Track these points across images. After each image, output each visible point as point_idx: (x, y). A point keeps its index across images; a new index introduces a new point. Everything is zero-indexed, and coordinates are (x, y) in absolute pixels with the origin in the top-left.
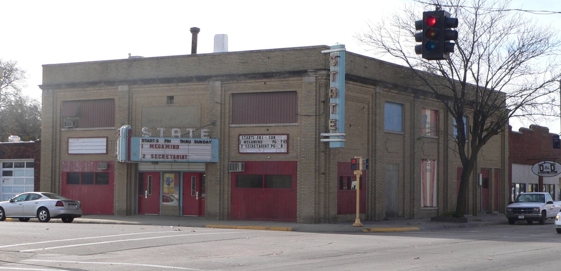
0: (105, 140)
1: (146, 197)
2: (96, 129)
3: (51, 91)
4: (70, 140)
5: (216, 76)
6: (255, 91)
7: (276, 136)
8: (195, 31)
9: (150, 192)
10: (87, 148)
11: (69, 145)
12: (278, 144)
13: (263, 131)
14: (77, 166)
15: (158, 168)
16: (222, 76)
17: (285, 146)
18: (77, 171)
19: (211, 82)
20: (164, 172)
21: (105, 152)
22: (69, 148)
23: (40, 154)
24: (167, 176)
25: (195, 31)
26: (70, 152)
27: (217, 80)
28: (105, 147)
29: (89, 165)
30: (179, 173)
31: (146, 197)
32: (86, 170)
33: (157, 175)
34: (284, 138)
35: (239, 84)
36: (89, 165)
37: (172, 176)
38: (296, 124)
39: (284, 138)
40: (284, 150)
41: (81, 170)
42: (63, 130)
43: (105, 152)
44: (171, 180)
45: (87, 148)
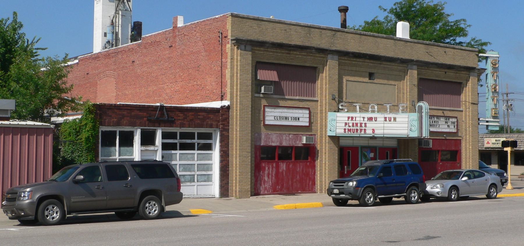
0: (308, 112)
1: (346, 173)
6: (437, 79)
13: (440, 113)
14: (274, 139)
18: (274, 144)
19: (409, 66)
22: (267, 118)
25: (344, 10)
26: (267, 123)
27: (415, 65)
31: (346, 173)
32: (284, 144)
33: (355, 149)
35: (427, 71)
36: (288, 138)
41: (278, 144)
43: (307, 124)
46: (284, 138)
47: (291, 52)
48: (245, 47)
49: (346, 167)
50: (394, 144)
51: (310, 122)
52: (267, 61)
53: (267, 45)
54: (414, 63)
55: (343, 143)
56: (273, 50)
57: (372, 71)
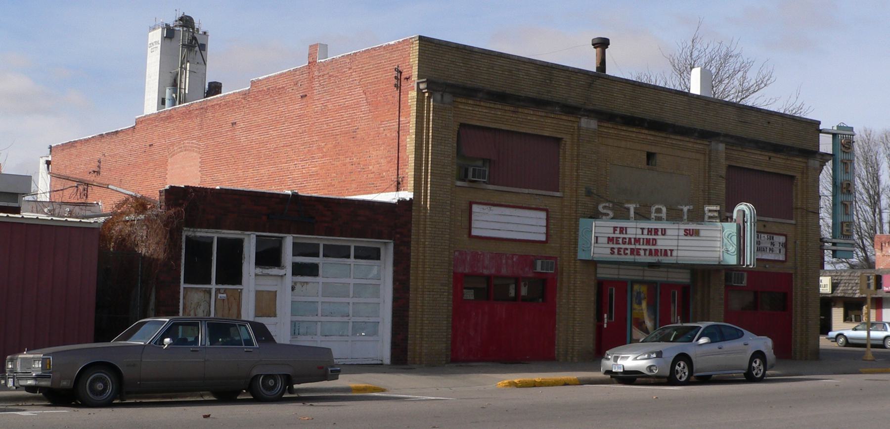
1: (605, 326)
2: (526, 191)
3: (448, 98)
4: (476, 208)
5: (726, 135)
6: (756, 168)
7: (775, 237)
8: (602, 44)
9: (610, 317)
10: (511, 227)
11: (474, 217)
12: (777, 248)
15: (625, 274)
16: (732, 137)
17: (783, 250)
19: (713, 143)
20: (633, 282)
21: (543, 238)
23: (410, 231)
24: (636, 287)
25: (602, 44)
26: (474, 232)
27: (722, 142)
28: (544, 230)
29: (510, 262)
30: (655, 283)
31: (605, 326)
33: (622, 286)
34: (782, 239)
36: (510, 262)
37: (644, 289)
38: (793, 222)
39: (782, 239)
40: (781, 257)
42: (459, 183)
43: (543, 238)
44: (642, 295)
45: (511, 227)
46: (504, 261)
47: (520, 110)
48: (442, 96)
49: (605, 316)
50: (684, 278)
51: (547, 234)
52: (478, 124)
53: (480, 95)
54: (721, 139)
55: (604, 273)
56: (488, 105)
57: (653, 149)
